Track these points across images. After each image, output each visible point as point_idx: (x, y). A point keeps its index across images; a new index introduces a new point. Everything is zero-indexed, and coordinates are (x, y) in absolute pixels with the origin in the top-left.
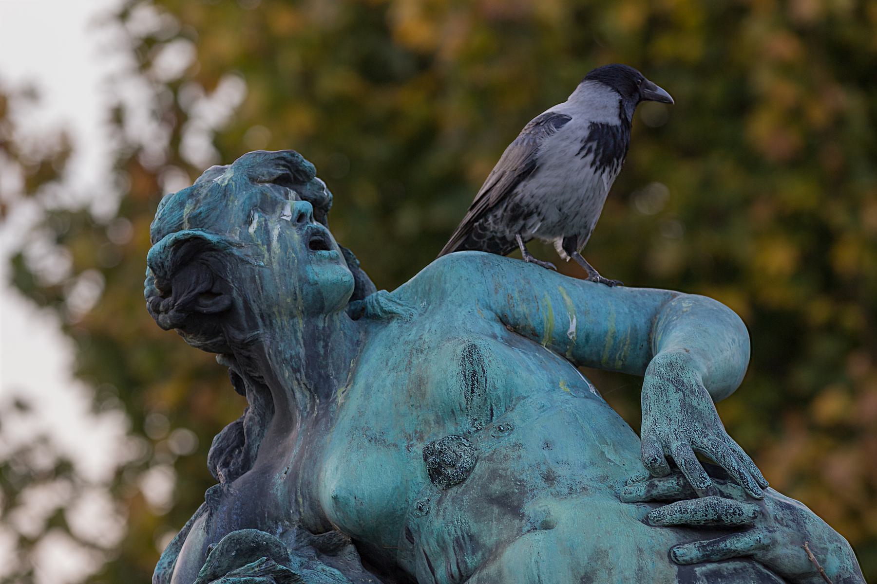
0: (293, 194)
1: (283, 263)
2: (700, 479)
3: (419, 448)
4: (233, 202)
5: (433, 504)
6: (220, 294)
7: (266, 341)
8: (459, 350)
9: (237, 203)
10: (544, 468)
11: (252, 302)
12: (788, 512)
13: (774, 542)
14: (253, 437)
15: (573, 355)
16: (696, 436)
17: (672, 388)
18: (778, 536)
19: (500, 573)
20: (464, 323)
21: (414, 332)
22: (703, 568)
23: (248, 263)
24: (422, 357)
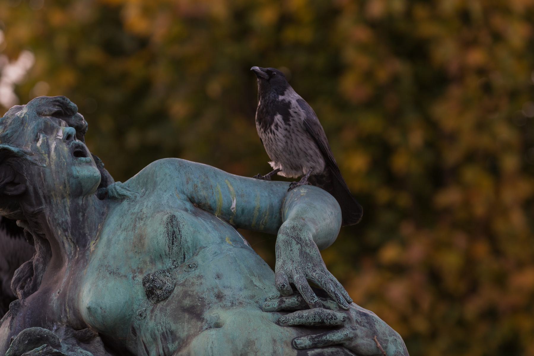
0: (64, 123)
1: (59, 165)
2: (311, 297)
3: (140, 278)
4: (27, 127)
5: (148, 312)
6: (19, 184)
7: (47, 212)
8: (165, 218)
9: (30, 128)
10: (216, 290)
11: (39, 189)
12: (364, 317)
13: (356, 336)
14: (39, 271)
15: (234, 221)
16: (309, 271)
17: (294, 242)
18: (358, 332)
20: (168, 202)
21: (137, 207)
22: (313, 352)
23: (36, 164)
24: (142, 223)
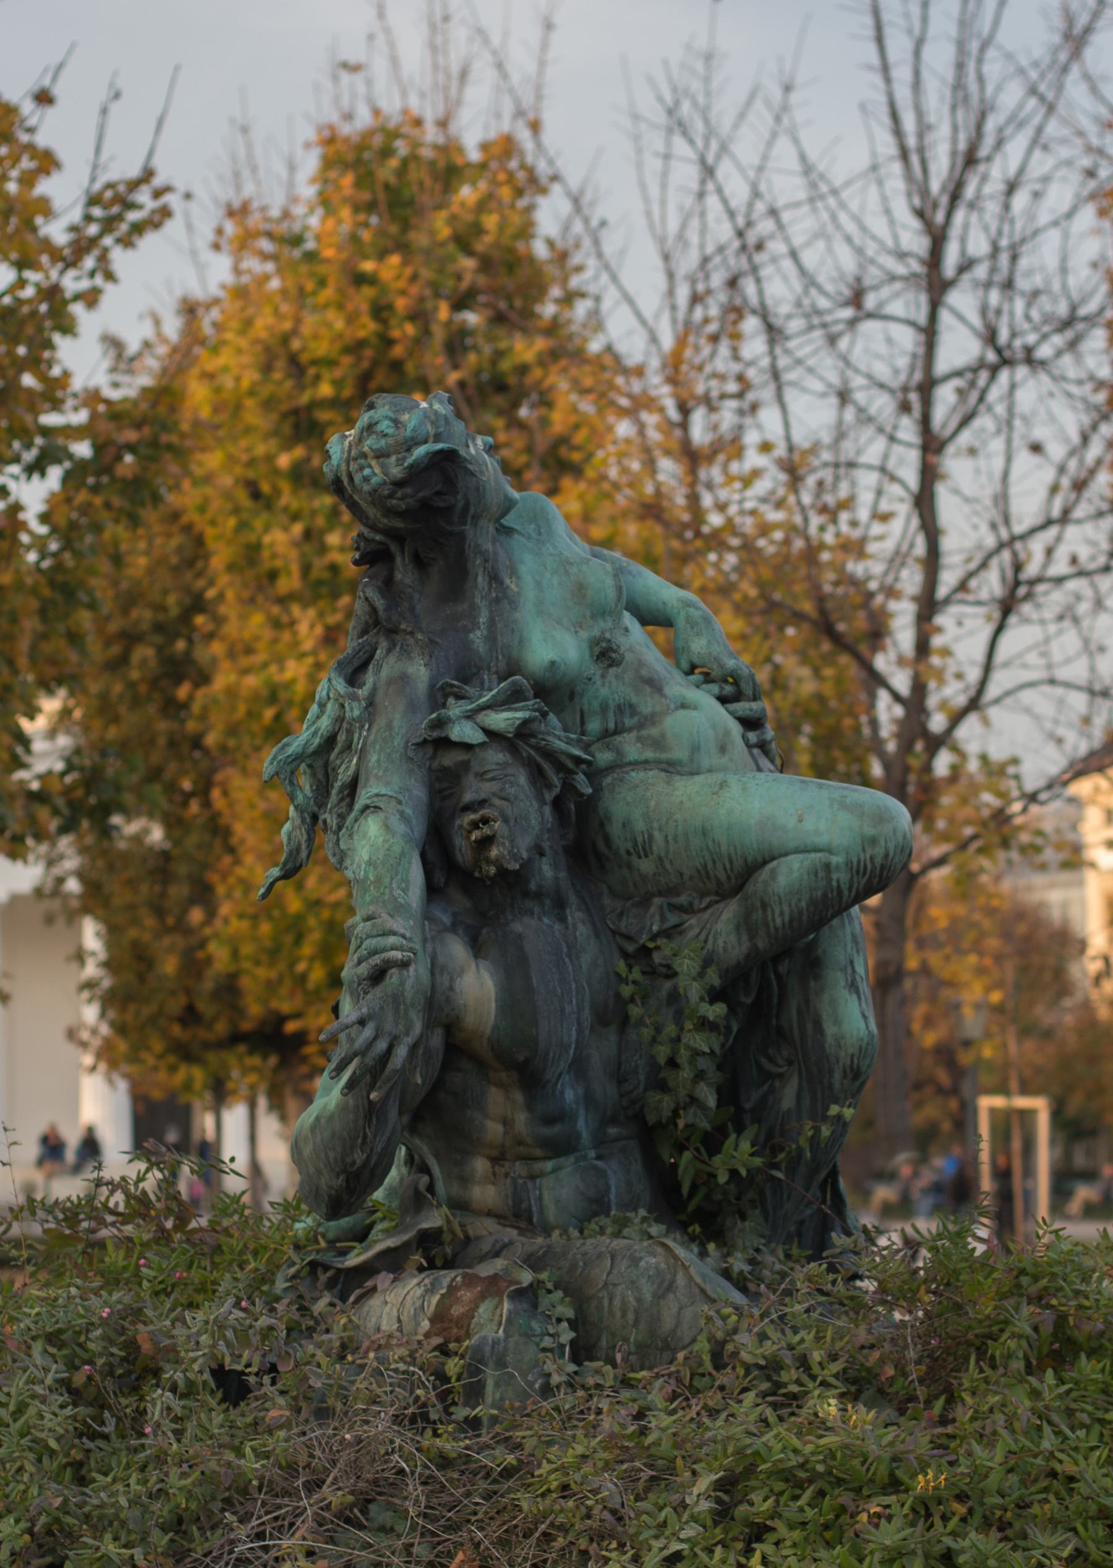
19: (663, 736)
